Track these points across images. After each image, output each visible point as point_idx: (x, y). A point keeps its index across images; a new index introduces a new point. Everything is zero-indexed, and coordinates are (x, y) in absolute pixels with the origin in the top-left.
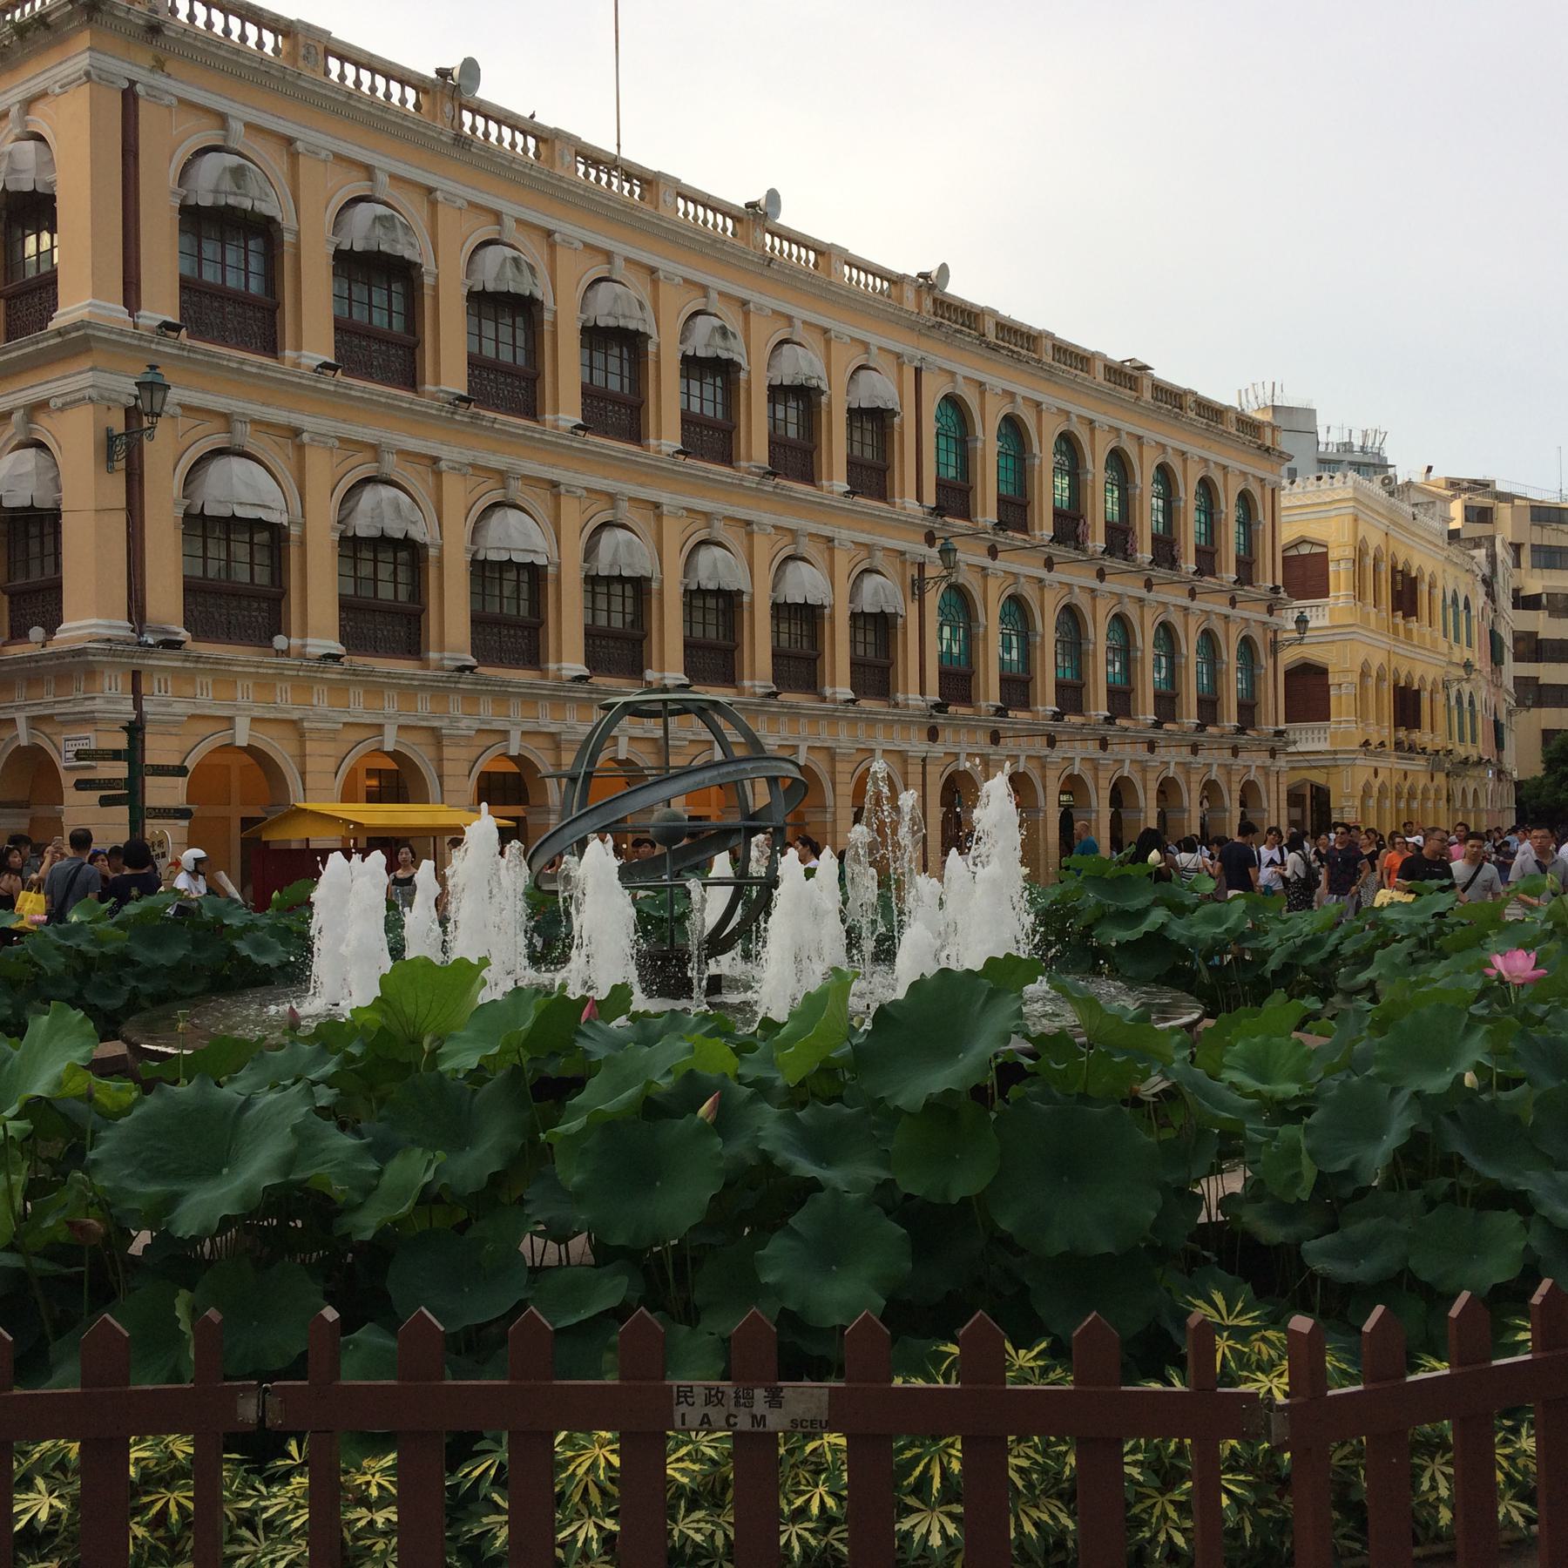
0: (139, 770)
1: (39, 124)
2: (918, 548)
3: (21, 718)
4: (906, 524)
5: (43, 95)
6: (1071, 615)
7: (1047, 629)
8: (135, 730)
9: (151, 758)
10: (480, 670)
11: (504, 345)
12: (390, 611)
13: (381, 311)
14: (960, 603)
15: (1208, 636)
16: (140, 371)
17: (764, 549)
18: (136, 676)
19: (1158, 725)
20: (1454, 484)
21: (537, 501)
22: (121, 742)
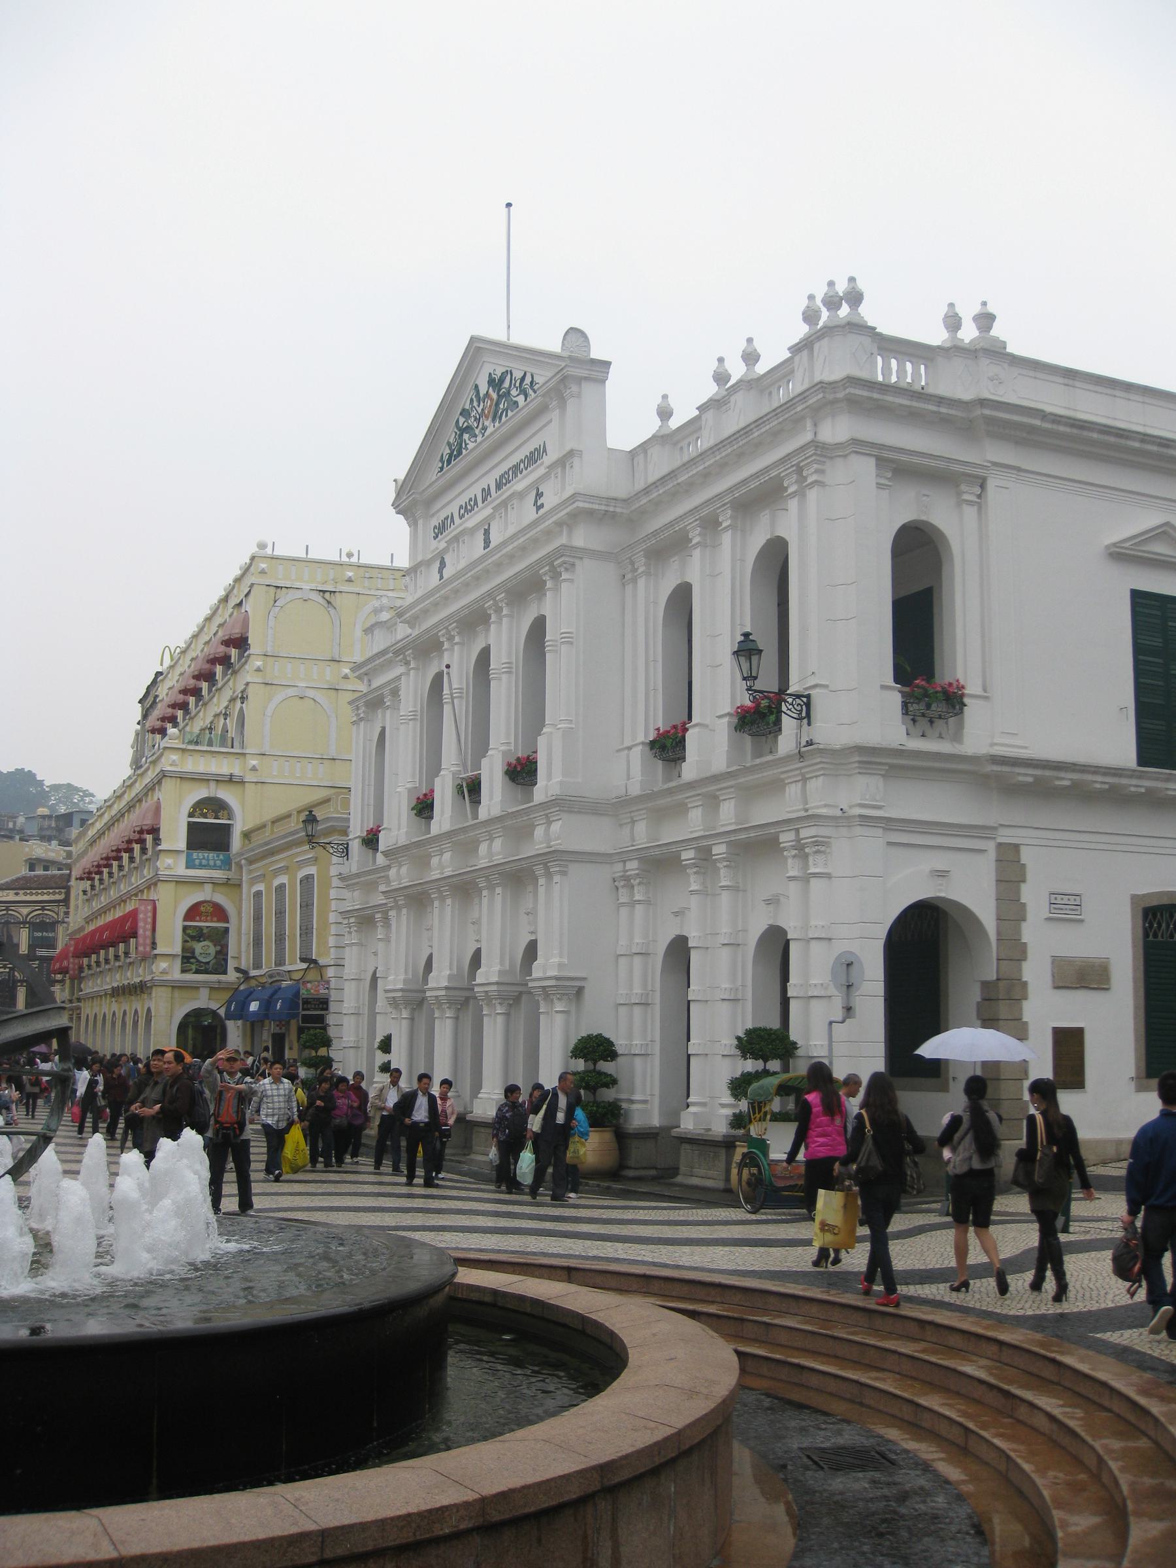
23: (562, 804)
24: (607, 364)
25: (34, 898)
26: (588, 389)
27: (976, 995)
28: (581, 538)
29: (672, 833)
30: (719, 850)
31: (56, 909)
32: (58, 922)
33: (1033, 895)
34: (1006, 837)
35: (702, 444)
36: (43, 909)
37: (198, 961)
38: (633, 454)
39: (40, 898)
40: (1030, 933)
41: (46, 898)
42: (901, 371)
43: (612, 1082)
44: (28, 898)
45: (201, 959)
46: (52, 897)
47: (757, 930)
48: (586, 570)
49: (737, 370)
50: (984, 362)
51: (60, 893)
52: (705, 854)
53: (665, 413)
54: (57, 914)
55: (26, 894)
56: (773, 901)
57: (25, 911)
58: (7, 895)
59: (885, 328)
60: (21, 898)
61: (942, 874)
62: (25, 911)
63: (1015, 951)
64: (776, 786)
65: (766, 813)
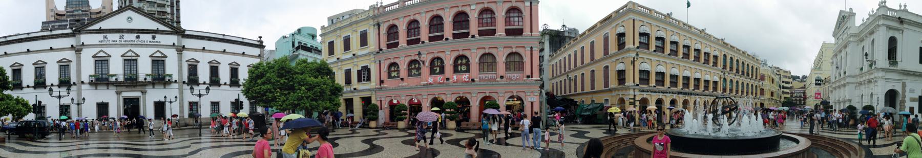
0: (635, 101)
1: (623, 24)
2: (720, 73)
3: (621, 94)
4: (719, 70)
5: (624, 21)
6: (737, 82)
7: (735, 84)
8: (635, 96)
9: (636, 99)
10: (640, 86)
11: (660, 44)
12: (645, 79)
13: (644, 40)
14: (725, 80)
15: (748, 84)
16: (636, 53)
17: (693, 71)
18: (634, 89)
19: (736, 94)
20: (775, 68)
21: (699, 71)
22: (633, 97)
23: (849, 76)
24: (855, 14)
26: (853, 17)
27: (899, 102)
28: (851, 39)
29: (862, 79)
30: (866, 82)
33: (907, 89)
34: (903, 81)
35: (867, 24)
38: (859, 27)
40: (906, 94)
42: (892, 14)
43: (855, 113)
47: (871, 93)
48: (852, 43)
49: (871, 13)
50: (904, 12)
52: (865, 83)
53: (863, 20)
56: (872, 89)
59: (889, 7)
61: (894, 86)
63: (904, 96)
64: (872, 74)
65: (872, 76)
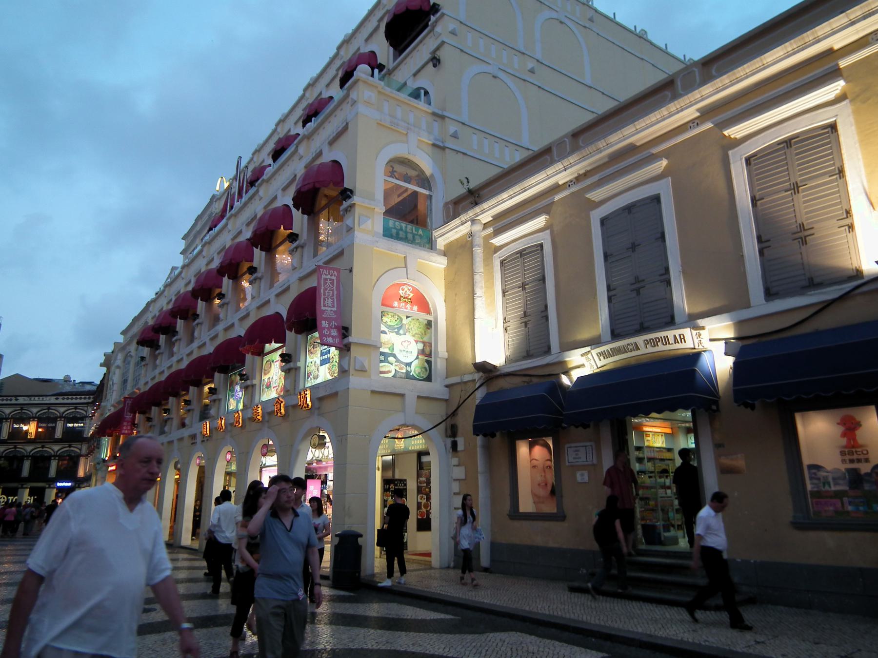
25: (69, 401)
31: (86, 409)
32: (86, 417)
36: (76, 408)
37: (398, 360)
39: (74, 401)
41: (78, 401)
44: (66, 401)
45: (400, 357)
46: (83, 401)
51: (89, 398)
54: (86, 412)
55: (63, 399)
57: (62, 410)
58: (50, 400)
60: (60, 401)
62: (62, 410)
